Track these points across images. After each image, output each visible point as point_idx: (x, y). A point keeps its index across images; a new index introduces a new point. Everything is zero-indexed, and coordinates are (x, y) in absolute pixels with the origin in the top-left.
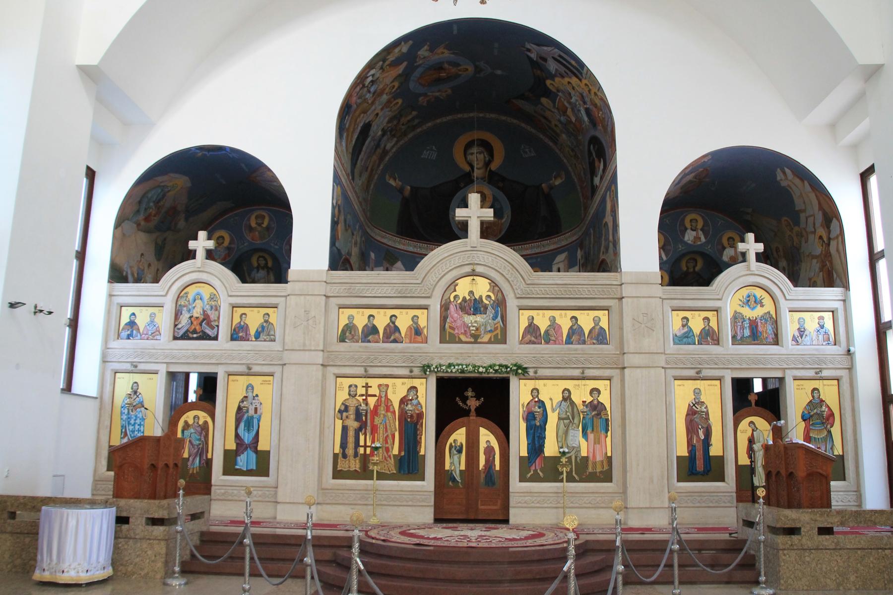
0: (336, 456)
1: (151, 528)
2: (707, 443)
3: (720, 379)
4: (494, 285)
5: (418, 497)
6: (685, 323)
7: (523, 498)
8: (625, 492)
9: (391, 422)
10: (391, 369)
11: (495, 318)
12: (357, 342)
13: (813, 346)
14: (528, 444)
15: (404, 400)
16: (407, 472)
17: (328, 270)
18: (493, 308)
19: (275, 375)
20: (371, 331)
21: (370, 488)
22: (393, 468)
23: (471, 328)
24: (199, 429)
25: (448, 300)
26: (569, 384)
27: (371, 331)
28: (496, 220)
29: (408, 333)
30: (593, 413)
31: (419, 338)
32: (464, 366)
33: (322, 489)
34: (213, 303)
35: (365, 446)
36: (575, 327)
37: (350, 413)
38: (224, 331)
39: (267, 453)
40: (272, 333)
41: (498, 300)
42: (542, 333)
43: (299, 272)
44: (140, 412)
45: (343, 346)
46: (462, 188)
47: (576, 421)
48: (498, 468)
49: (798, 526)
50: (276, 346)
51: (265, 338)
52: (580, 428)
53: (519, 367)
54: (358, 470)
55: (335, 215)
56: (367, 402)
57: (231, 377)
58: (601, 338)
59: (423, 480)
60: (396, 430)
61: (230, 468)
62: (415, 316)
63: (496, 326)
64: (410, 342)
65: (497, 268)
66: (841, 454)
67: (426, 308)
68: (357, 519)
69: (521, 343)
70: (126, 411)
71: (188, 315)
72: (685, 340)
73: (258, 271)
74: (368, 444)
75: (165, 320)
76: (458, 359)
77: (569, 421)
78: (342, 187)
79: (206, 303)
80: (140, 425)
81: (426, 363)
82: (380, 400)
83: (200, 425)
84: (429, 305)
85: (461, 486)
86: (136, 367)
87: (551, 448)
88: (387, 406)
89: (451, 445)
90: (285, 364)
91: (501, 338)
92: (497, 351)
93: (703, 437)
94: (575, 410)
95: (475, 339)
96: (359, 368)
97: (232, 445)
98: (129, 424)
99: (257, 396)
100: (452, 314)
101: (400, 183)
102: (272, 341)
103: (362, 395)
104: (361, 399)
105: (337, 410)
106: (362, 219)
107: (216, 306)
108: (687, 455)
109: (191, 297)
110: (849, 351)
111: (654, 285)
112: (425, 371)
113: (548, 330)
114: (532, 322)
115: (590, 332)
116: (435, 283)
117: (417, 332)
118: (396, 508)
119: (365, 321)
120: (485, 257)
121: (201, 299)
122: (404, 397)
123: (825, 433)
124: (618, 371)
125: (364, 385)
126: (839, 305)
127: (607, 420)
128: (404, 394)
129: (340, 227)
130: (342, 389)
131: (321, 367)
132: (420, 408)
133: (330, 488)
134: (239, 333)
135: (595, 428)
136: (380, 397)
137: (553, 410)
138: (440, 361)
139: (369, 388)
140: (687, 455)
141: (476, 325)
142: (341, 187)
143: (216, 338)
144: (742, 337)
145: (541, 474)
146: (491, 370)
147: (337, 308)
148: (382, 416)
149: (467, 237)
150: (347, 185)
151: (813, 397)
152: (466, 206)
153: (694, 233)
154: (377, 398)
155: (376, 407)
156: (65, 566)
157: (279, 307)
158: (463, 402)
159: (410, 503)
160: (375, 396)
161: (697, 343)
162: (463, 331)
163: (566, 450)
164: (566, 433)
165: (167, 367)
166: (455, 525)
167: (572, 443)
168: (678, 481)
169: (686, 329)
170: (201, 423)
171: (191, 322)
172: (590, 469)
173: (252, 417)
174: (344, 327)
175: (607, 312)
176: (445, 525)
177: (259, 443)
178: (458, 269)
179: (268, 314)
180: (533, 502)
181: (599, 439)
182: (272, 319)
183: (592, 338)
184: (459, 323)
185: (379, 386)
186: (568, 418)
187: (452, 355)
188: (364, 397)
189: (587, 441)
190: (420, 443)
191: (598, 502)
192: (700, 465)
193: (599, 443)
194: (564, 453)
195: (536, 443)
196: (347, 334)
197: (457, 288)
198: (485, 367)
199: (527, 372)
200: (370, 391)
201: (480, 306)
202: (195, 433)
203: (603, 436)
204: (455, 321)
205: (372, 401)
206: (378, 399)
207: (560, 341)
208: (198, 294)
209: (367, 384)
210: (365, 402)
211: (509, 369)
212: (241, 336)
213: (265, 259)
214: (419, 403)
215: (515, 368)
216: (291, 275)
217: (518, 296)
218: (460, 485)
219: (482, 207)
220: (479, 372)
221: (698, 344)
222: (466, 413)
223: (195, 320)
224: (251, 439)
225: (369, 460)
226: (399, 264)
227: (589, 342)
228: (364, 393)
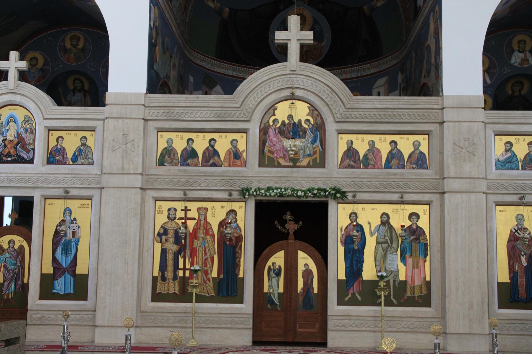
0: (155, 279)
4: (313, 109)
5: (237, 319)
6: (508, 148)
7: (340, 321)
8: (443, 317)
9: (210, 245)
10: (210, 192)
11: (314, 142)
12: (177, 165)
14: (346, 268)
15: (223, 224)
16: (226, 295)
17: (147, 93)
18: (312, 132)
19: (94, 199)
21: (189, 310)
22: (212, 291)
23: (290, 152)
24: (14, 254)
25: (267, 124)
26: (387, 209)
28: (316, 43)
29: (227, 157)
30: (412, 238)
31: (238, 162)
32: (283, 190)
33: (140, 311)
34: (28, 126)
35: (184, 269)
36: (394, 152)
37: (170, 236)
38: (40, 155)
40: (90, 156)
41: (317, 124)
42: (361, 156)
45: (162, 170)
46: (281, 11)
47: (394, 245)
48: (316, 291)
50: (94, 170)
51: (83, 161)
52: (399, 252)
53: (338, 191)
54: (177, 292)
55: (153, 37)
56: (186, 225)
57: (48, 201)
58: (421, 162)
59: (242, 303)
60: (215, 253)
62: (234, 140)
63: (315, 150)
64: (229, 166)
65: (315, 92)
67: (245, 131)
68: (176, 341)
69: (340, 167)
71: (2, 138)
72: (507, 165)
73: (74, 94)
74: (188, 267)
76: (276, 182)
77: (387, 245)
78: (160, 8)
79: (20, 126)
81: (244, 186)
82: (199, 224)
83: (15, 249)
84: (248, 129)
85: (279, 309)
88: (206, 229)
89: (269, 267)
90: (103, 188)
92: (317, 175)
94: (394, 234)
95: (294, 163)
96: (179, 192)
97: (48, 269)
99: (75, 219)
100: (271, 138)
101: (219, 5)
102: (90, 164)
103: (182, 219)
104: (180, 222)
105: (156, 233)
106: (180, 41)
107: (31, 129)
108: (509, 281)
111: (477, 110)
112: (244, 195)
113: (367, 155)
114: (351, 147)
115: (410, 156)
116: (254, 107)
118: (214, 330)
119: (184, 145)
120: (305, 80)
121: (15, 122)
122: (223, 220)
124: (437, 196)
125: (183, 208)
127: (426, 245)
128: (223, 217)
129: (158, 49)
130: (161, 212)
131: (139, 190)
132: (239, 231)
133: (149, 311)
135: (413, 252)
136: (199, 220)
137: (372, 234)
138: (259, 185)
139: (188, 212)
140: (509, 281)
141: (295, 149)
142: (159, 8)
143: (31, 162)
145: (359, 298)
146: (310, 194)
147: (156, 132)
149: (286, 60)
150: (165, 5)
152: (286, 29)
153: (522, 55)
154: (196, 221)
155: (195, 230)
157: (97, 130)
159: (229, 326)
160: (194, 219)
161: (520, 168)
162: (282, 155)
163: (385, 274)
164: (384, 257)
166: (273, 348)
167: (390, 267)
169: (509, 154)
170: (16, 247)
171: (5, 145)
172: (408, 294)
173: (70, 241)
174: (163, 150)
175: (427, 136)
176: (263, 348)
177: (77, 267)
178: (278, 93)
179: (85, 138)
180: (351, 325)
181: (418, 263)
182: (90, 143)
183: (411, 163)
184: (278, 147)
185: (199, 209)
186: (386, 242)
187: (270, 178)
188: (183, 221)
189: (405, 265)
190: (240, 266)
191: (416, 327)
193: (417, 268)
194: (382, 277)
195: (354, 266)
196: (166, 158)
197: (276, 112)
200: (190, 215)
201: (300, 130)
202: (10, 257)
203: (421, 261)
204: (274, 145)
205: (191, 224)
206: (197, 223)
207: (379, 165)
208: (12, 116)
209: (186, 207)
210: (184, 225)
211: (327, 193)
212: (58, 160)
213: (82, 82)
214: (238, 227)
215: (334, 192)
216: (109, 98)
217: (337, 120)
218: (278, 307)
219: (302, 30)
220: (297, 196)
221: (522, 169)
222: (285, 236)
223: (9, 143)
224: (69, 262)
225: (188, 282)
226: (218, 88)
227: (408, 167)
228: (183, 216)
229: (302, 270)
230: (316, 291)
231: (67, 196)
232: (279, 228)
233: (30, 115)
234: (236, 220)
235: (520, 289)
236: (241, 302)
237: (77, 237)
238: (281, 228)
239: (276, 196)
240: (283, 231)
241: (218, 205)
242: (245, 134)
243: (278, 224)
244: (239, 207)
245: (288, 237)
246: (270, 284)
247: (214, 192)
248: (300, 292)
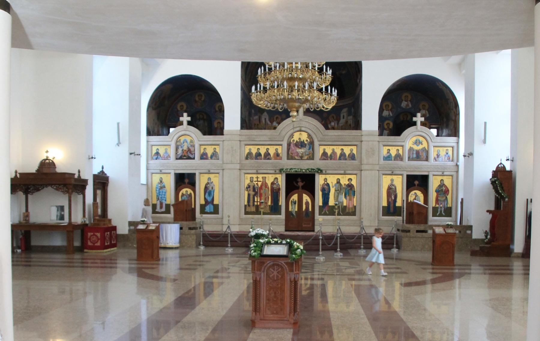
0: (245, 206)
1: (190, 231)
2: (395, 201)
3: (402, 175)
4: (309, 136)
11: (309, 149)
12: (253, 159)
13: (443, 162)
20: (258, 155)
22: (269, 210)
24: (188, 196)
27: (258, 155)
30: (349, 188)
31: (278, 158)
32: (297, 169)
33: (241, 219)
35: (257, 202)
36: (342, 153)
38: (197, 156)
39: (218, 205)
40: (217, 156)
42: (329, 155)
43: (228, 131)
44: (164, 190)
47: (342, 191)
48: (310, 210)
49: (409, 229)
50: (220, 162)
53: (319, 169)
57: (202, 175)
60: (269, 195)
61: (203, 211)
66: (451, 206)
67: (281, 145)
69: (320, 159)
70: (158, 190)
72: (388, 159)
75: (172, 152)
79: (189, 144)
80: (164, 195)
86: (161, 171)
87: (331, 202)
89: (292, 201)
91: (312, 158)
93: (393, 198)
94: (342, 187)
95: (301, 158)
97: (203, 202)
98: (160, 194)
99: (212, 182)
103: (256, 181)
105: (245, 187)
107: (193, 145)
109: (182, 141)
110: (457, 164)
112: (281, 172)
114: (325, 151)
115: (349, 155)
117: (277, 155)
121: (186, 142)
122: (273, 182)
123: (445, 198)
124: (359, 172)
126: (455, 145)
127: (354, 191)
130: (247, 179)
131: (239, 170)
134: (204, 156)
137: (333, 187)
143: (194, 159)
144: (412, 158)
145: (327, 212)
146: (308, 171)
148: (264, 190)
151: (441, 183)
153: (406, 103)
155: (261, 186)
156: (168, 242)
158: (296, 184)
160: (261, 181)
161: (393, 160)
163: (337, 203)
164: (338, 196)
165: (174, 171)
168: (383, 216)
169: (389, 154)
170: (189, 193)
172: (347, 211)
179: (215, 148)
182: (217, 150)
183: (349, 158)
185: (263, 178)
186: (339, 190)
189: (346, 199)
192: (392, 210)
194: (336, 204)
197: (294, 137)
198: (305, 170)
199: (322, 172)
200: (259, 180)
205: (260, 184)
208: (185, 140)
209: (257, 177)
211: (315, 171)
214: (279, 184)
215: (317, 170)
216: (225, 133)
217: (319, 140)
222: (298, 188)
228: (256, 180)
230: (310, 210)
231: (209, 173)
233: (192, 139)
234: (278, 182)
235: (391, 208)
236: (280, 214)
237: (213, 189)
241: (270, 175)
242: (281, 146)
244: (279, 176)
247: (269, 171)
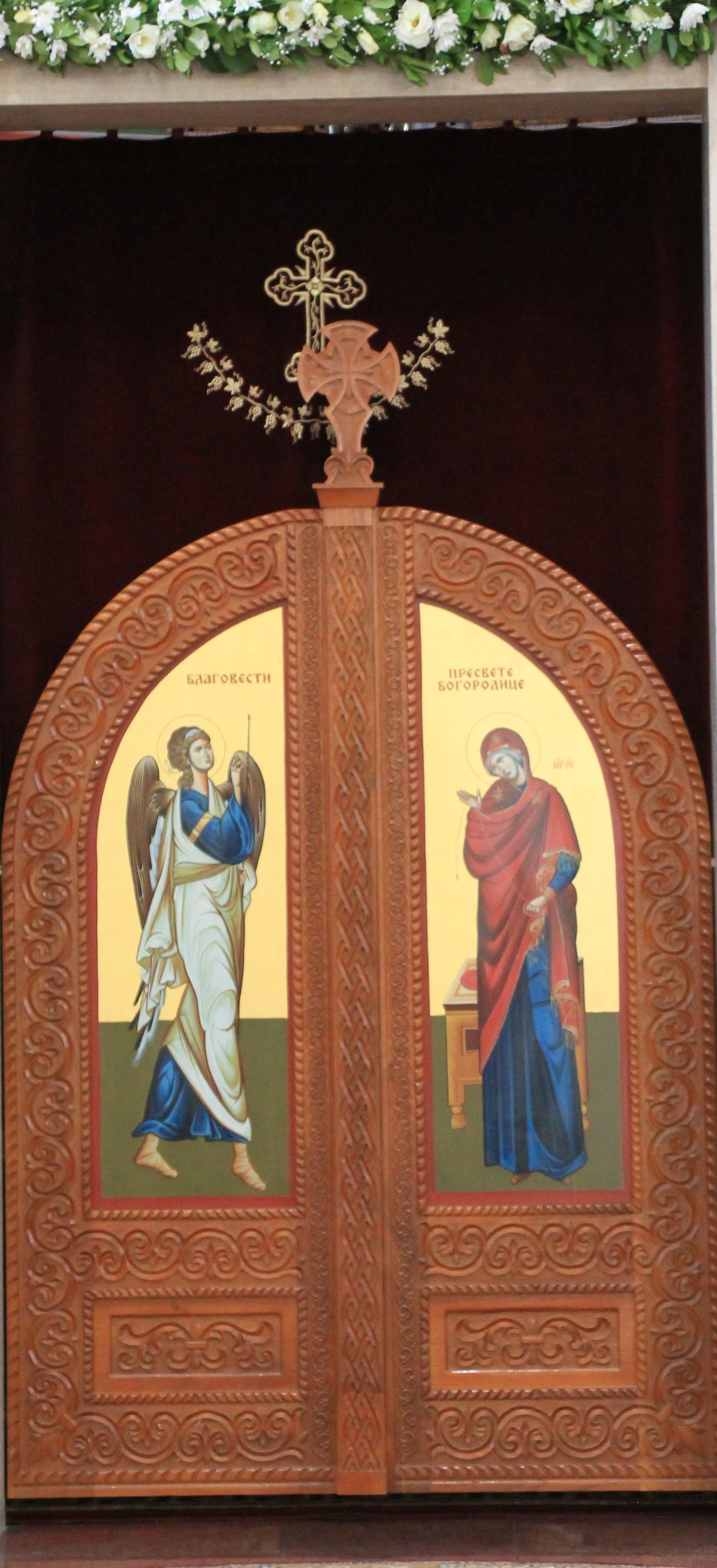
85: (254, 1179)
218: (244, 1165)
229: (464, 796)
232: (224, 396)
238: (244, 390)
239: (183, 64)
240: (271, 421)
243: (217, 357)
245: (323, 478)
246: (155, 943)
248: (448, 1007)
